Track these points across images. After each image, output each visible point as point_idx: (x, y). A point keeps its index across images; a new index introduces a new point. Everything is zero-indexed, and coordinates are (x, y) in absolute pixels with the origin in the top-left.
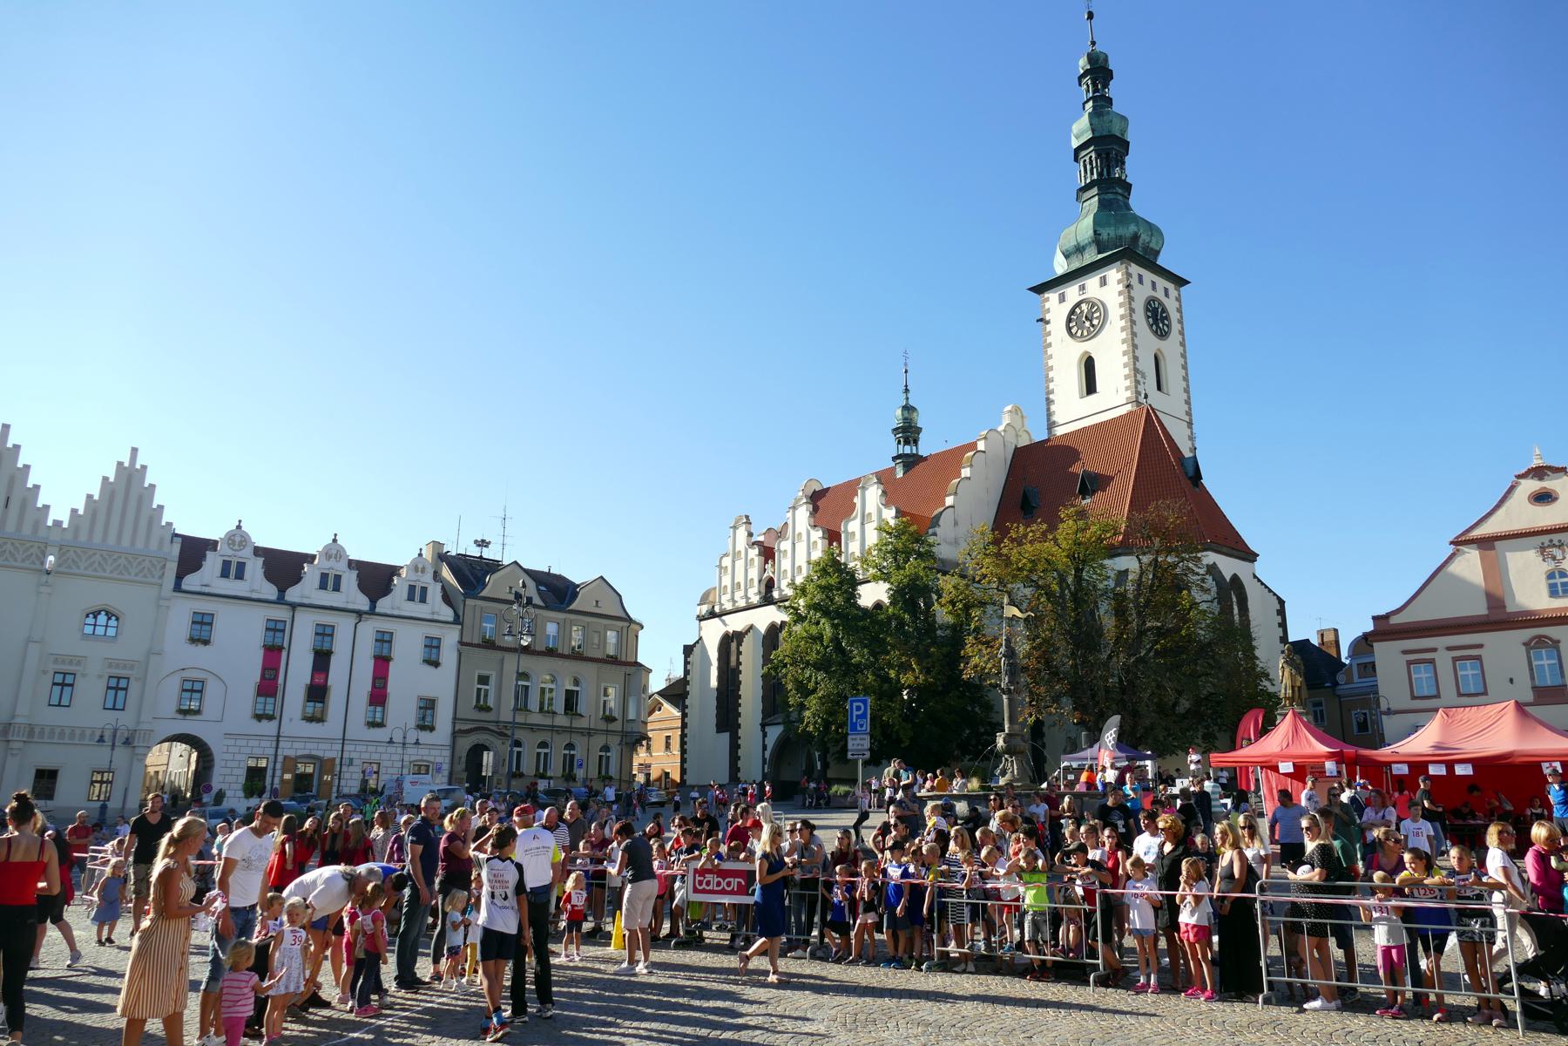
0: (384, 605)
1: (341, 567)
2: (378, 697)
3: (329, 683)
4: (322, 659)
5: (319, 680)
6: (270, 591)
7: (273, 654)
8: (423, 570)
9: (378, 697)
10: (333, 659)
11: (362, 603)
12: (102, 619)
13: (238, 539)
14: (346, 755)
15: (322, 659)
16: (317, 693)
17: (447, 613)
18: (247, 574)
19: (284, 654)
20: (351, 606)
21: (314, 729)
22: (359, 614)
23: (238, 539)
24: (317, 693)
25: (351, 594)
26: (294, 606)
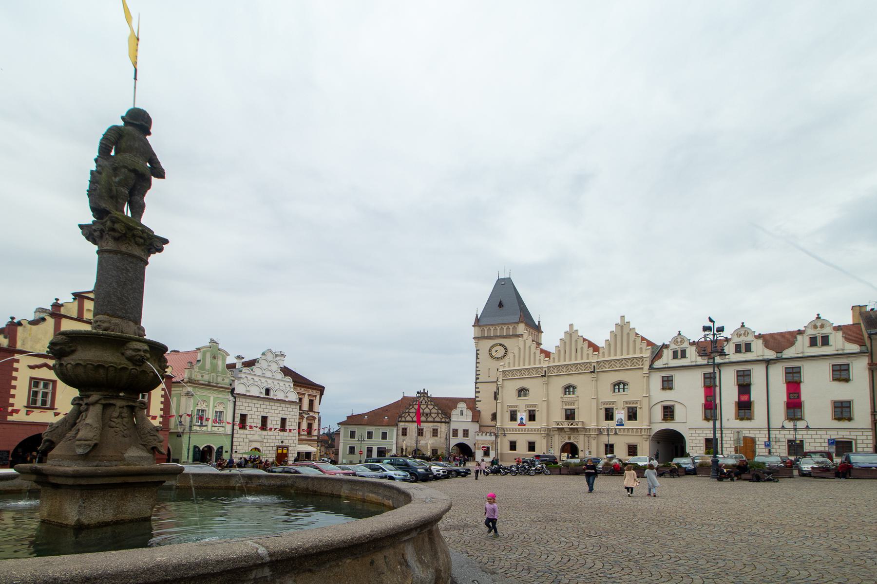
0: (789, 353)
1: (749, 338)
2: (794, 406)
3: (752, 399)
4: (744, 388)
5: (744, 398)
6: (701, 361)
7: (711, 387)
8: (822, 326)
9: (794, 406)
10: (753, 388)
11: (770, 354)
12: (622, 386)
13: (679, 340)
14: (772, 436)
15: (744, 388)
16: (744, 407)
17: (854, 348)
18: (687, 355)
19: (717, 389)
20: (761, 358)
21: (745, 424)
22: (768, 362)
23: (679, 340)
24: (744, 407)
25: (759, 350)
26: (719, 365)
